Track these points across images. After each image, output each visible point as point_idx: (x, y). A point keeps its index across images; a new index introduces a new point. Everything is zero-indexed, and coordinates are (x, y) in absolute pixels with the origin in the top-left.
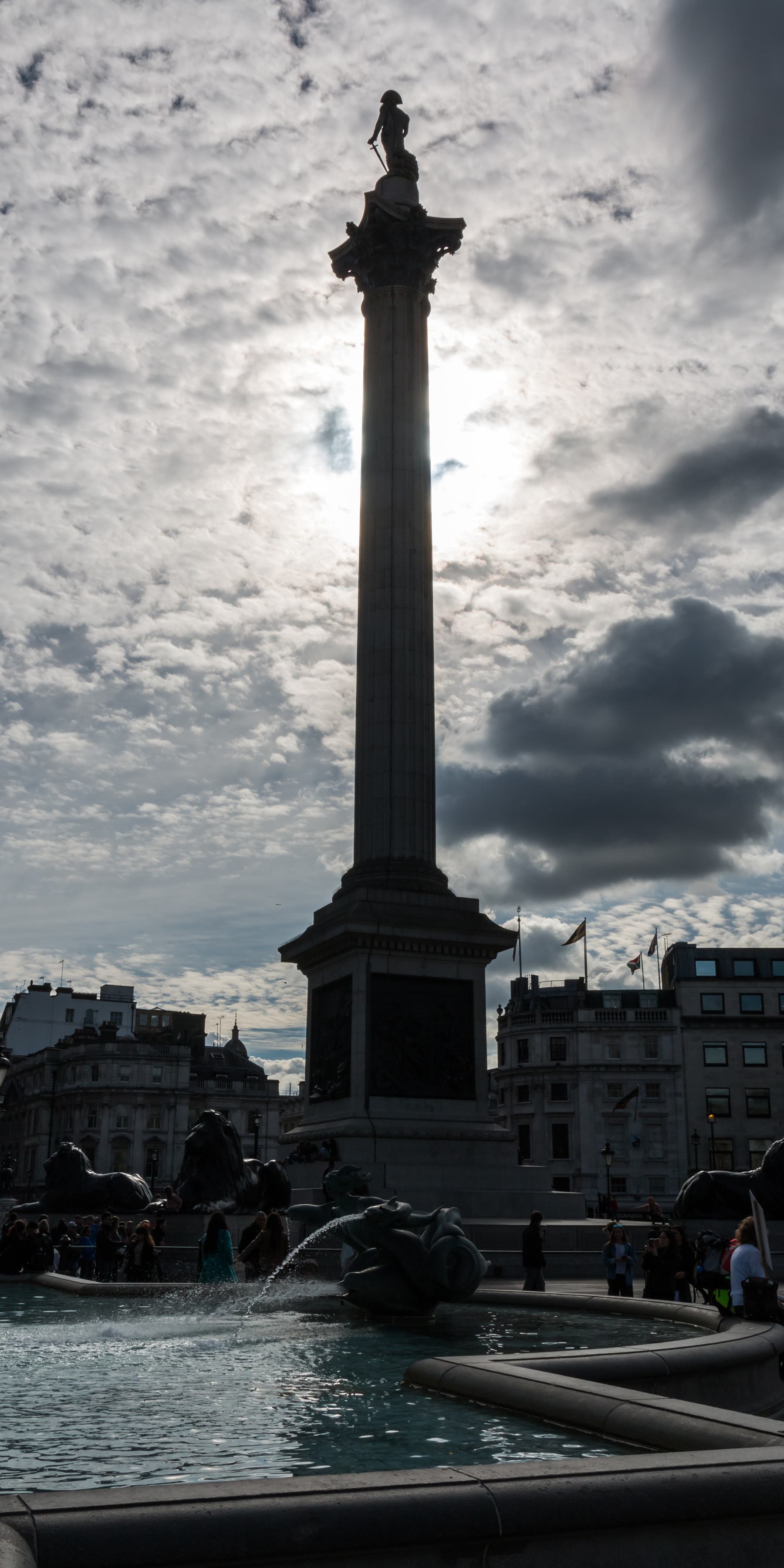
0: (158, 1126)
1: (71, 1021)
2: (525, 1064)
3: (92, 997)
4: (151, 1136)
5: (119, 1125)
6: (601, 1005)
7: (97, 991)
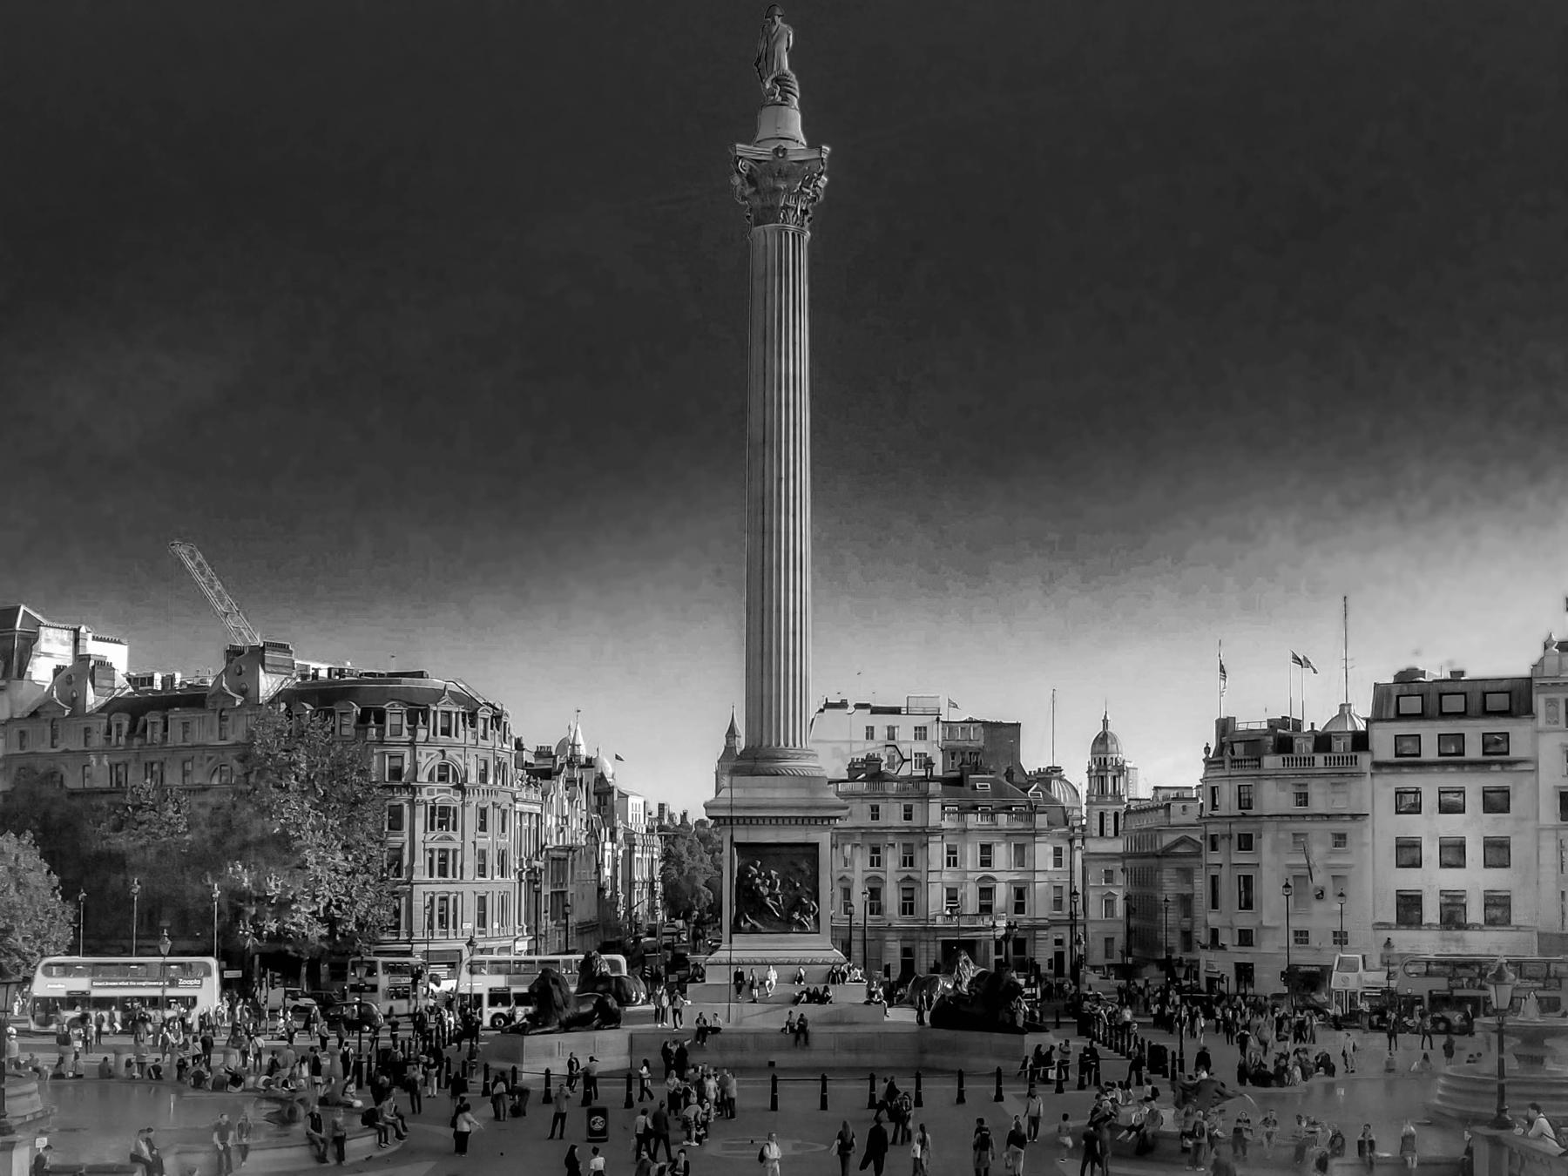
0: (911, 865)
1: (872, 738)
2: (1215, 813)
3: (896, 711)
4: (905, 875)
5: (872, 865)
6: (1291, 750)
7: (903, 704)
